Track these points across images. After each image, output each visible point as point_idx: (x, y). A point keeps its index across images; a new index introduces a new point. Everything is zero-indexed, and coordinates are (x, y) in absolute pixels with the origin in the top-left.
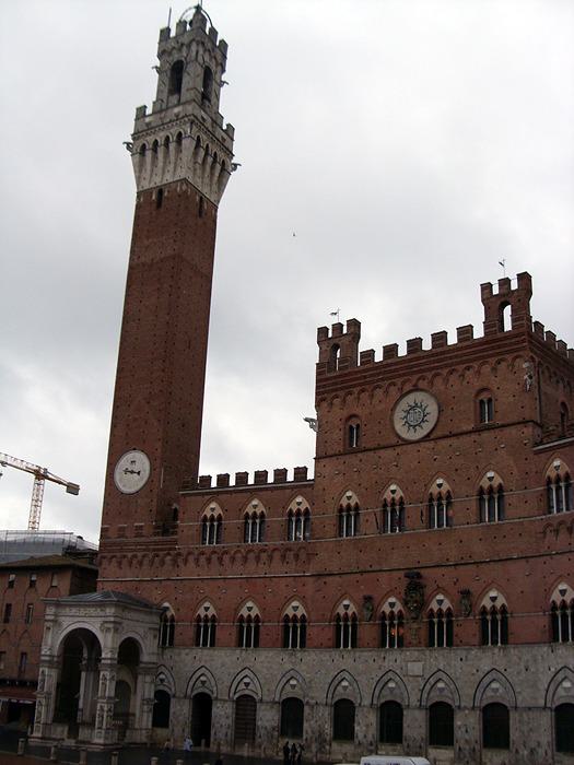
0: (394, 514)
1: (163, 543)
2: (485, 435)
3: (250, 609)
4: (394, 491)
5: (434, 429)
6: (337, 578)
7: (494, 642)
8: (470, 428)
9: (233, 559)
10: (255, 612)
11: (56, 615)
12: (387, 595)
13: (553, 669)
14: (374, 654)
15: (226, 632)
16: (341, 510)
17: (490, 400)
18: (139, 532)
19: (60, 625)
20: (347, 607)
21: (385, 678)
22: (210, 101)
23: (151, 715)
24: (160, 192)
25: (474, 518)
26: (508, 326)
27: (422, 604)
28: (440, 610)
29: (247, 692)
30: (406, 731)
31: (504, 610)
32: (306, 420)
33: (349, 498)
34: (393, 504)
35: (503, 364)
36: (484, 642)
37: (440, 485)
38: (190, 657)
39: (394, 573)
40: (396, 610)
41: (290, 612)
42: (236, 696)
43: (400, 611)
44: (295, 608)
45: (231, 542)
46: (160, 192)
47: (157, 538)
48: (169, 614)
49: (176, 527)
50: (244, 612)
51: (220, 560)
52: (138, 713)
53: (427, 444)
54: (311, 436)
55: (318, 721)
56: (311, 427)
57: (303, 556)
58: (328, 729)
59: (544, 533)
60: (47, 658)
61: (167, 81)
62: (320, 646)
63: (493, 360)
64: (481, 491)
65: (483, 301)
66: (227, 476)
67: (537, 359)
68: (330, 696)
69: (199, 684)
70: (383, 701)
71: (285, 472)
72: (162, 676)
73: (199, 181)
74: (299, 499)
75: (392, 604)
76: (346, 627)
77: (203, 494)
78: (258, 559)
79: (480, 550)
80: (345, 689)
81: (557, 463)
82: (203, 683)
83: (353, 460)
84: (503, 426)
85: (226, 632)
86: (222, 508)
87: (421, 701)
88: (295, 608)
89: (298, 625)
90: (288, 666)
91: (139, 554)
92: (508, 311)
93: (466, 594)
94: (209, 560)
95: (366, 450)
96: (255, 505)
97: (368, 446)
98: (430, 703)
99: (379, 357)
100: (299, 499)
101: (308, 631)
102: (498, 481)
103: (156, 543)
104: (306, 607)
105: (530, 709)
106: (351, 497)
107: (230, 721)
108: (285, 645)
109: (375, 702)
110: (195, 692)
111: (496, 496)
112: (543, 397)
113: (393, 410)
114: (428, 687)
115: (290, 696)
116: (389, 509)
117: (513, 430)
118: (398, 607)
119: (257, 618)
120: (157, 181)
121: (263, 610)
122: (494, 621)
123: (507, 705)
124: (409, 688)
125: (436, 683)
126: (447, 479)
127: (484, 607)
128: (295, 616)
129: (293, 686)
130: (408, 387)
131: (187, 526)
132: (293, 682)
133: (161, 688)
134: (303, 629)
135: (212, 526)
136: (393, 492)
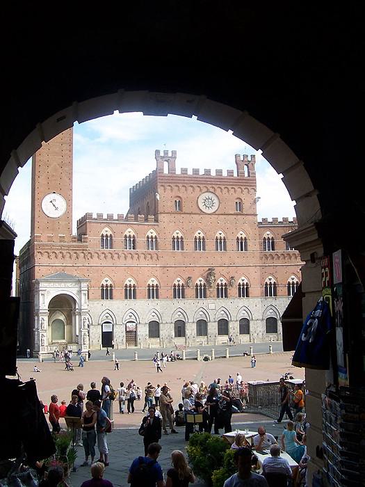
0: (200, 243)
2: (239, 216)
4: (199, 234)
10: (133, 283)
12: (198, 277)
14: (194, 301)
16: (174, 238)
20: (179, 281)
25: (236, 249)
30: (209, 331)
33: (177, 233)
34: (200, 239)
37: (220, 234)
44: (153, 281)
47: (74, 244)
49: (86, 238)
51: (112, 257)
55: (167, 330)
75: (200, 281)
79: (238, 262)
81: (268, 233)
85: (118, 292)
88: (153, 281)
91: (63, 251)
97: (186, 212)
102: (244, 236)
129: (153, 316)
130: (206, 190)
131: (93, 238)
134: (157, 290)
136: (199, 233)
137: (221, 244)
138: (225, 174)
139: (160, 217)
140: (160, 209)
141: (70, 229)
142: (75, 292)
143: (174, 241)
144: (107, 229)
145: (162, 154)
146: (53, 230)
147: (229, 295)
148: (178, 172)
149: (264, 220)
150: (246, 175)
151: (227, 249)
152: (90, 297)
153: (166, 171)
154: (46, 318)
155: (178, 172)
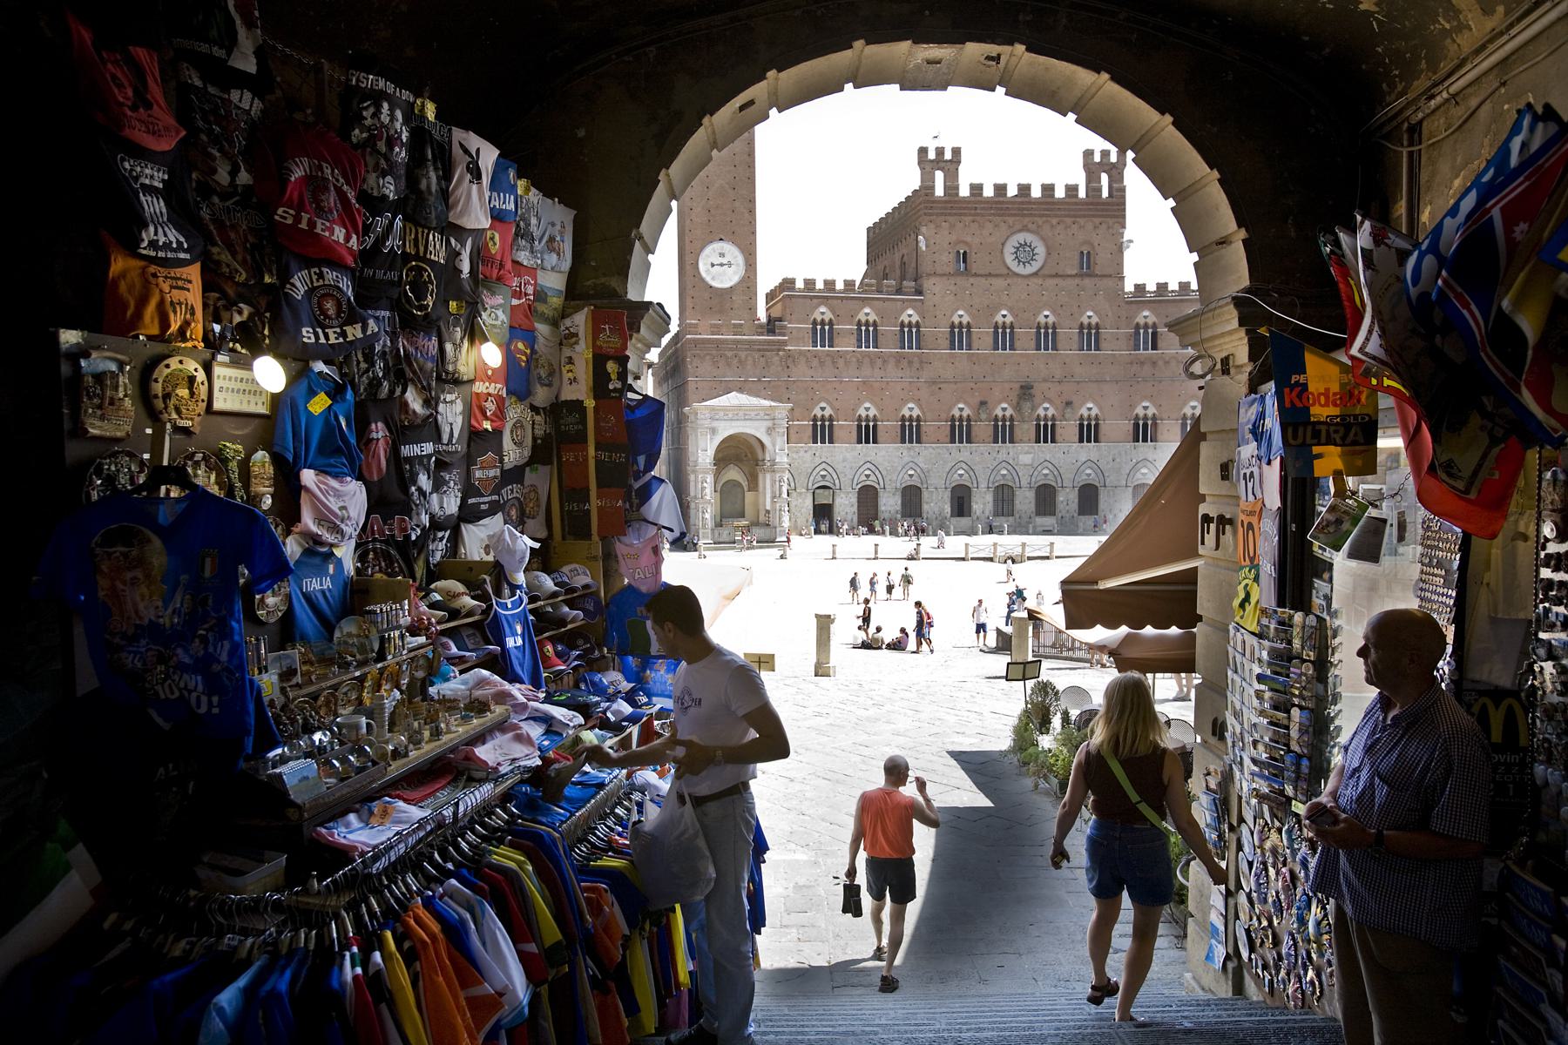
0: (1004, 337)
1: (769, 342)
2: (1087, 282)
3: (867, 409)
4: (1004, 316)
6: (953, 386)
7: (1089, 441)
16: (953, 326)
18: (737, 329)
19: (714, 431)
20: (961, 410)
25: (1076, 346)
27: (1034, 408)
31: (1097, 418)
34: (1004, 327)
35: (1104, 226)
36: (1081, 441)
37: (1046, 316)
38: (810, 453)
39: (1007, 386)
40: (1008, 414)
44: (911, 409)
45: (846, 346)
53: (1035, 280)
57: (916, 365)
58: (948, 509)
62: (938, 441)
63: (1097, 220)
64: (1081, 326)
65: (1085, 166)
66: (833, 283)
74: (910, 312)
75: (1004, 409)
77: (812, 298)
80: (960, 476)
81: (1146, 313)
82: (823, 477)
83: (960, 281)
90: (907, 459)
95: (976, 275)
99: (988, 192)
101: (923, 429)
102: (1095, 320)
103: (760, 342)
104: (920, 407)
106: (962, 316)
107: (855, 509)
108: (903, 442)
117: (1109, 283)
119: (875, 419)
121: (881, 410)
126: (1054, 312)
130: (1018, 227)
134: (918, 426)
135: (823, 330)
137: (1046, 337)
138: (1060, 193)
139: (928, 284)
140: (926, 267)
141: (753, 309)
142: (763, 430)
143: (952, 332)
144: (823, 309)
145: (932, 155)
146: (721, 312)
147: (1058, 437)
148: (964, 192)
149: (1137, 286)
150: (1105, 194)
151: (1059, 346)
152: (793, 436)
153: (939, 191)
154: (710, 479)
155: (964, 192)
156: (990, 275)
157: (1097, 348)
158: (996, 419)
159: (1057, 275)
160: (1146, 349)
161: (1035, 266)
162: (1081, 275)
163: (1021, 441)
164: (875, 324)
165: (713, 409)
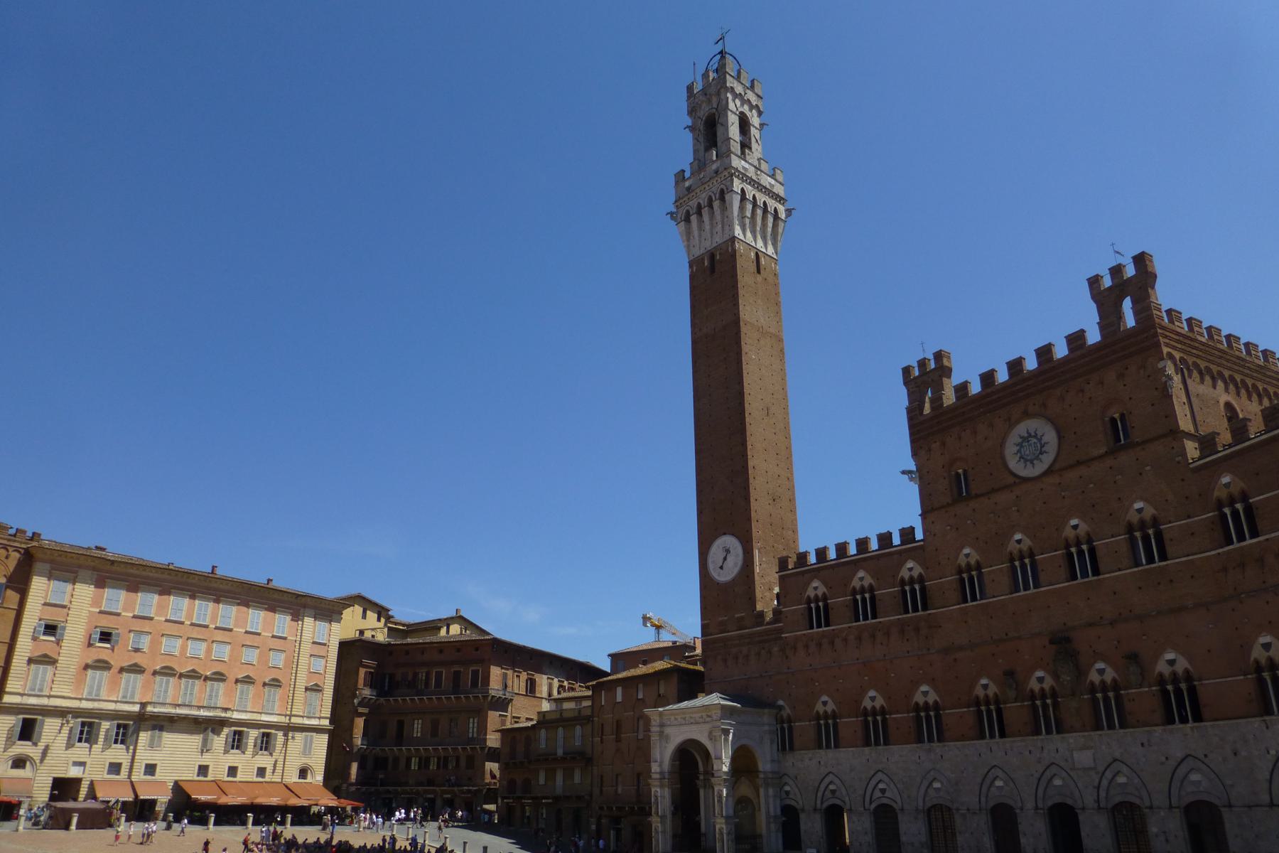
0: (1024, 570)
3: (873, 699)
5: (1055, 461)
7: (1184, 720)
8: (1103, 450)
9: (845, 640)
11: (662, 725)
12: (1033, 669)
13: (1273, 752)
15: (849, 724)
16: (960, 572)
17: (1122, 416)
20: (985, 687)
21: (1048, 774)
22: (750, 148)
23: (780, 835)
24: (712, 256)
26: (1130, 321)
27: (1081, 673)
28: (1103, 682)
29: (885, 801)
31: (1188, 677)
32: (904, 472)
33: (967, 555)
34: (1022, 558)
36: (1170, 721)
41: (919, 698)
42: (873, 806)
43: (1052, 688)
44: (925, 694)
46: (712, 256)
48: (785, 715)
49: (780, 612)
50: (867, 703)
51: (832, 643)
52: (764, 832)
54: (914, 489)
56: (911, 479)
59: (1225, 570)
60: (658, 776)
61: (701, 139)
62: (963, 738)
64: (1130, 529)
65: (1093, 297)
67: (1177, 355)
68: (983, 799)
69: (828, 794)
70: (1050, 803)
71: (889, 535)
72: (787, 788)
73: (749, 234)
75: (1040, 679)
76: (989, 712)
78: (873, 636)
81: (1226, 479)
82: (833, 792)
84: (1144, 442)
86: (825, 583)
87: (1098, 801)
88: (925, 694)
89: (932, 713)
92: (1127, 304)
93: (1133, 657)
94: (819, 645)
95: (977, 496)
96: (862, 578)
98: (1110, 806)
100: (910, 564)
102: (1150, 511)
105: (1249, 807)
108: (920, 740)
109: (1040, 805)
110: (825, 805)
111: (1151, 532)
112: (1193, 399)
113: (1002, 445)
114: (1105, 783)
115: (935, 802)
116: (1017, 563)
118: (1049, 683)
119: (883, 711)
120: (708, 245)
122: (1178, 692)
123: (1216, 802)
124: (1080, 785)
125: (1114, 776)
127: (1161, 675)
128: (926, 703)
129: (937, 790)
132: (937, 785)
133: (788, 802)
134: (938, 717)
136: (1019, 542)
144: (815, 583)
148: (949, 398)
151: (1102, 567)
155: (949, 398)
156: (994, 491)
157: (1163, 557)
158: (1032, 696)
159: (1079, 463)
160: (1241, 538)
161: (1047, 459)
162: (1112, 452)
163: (1072, 730)
164: (871, 589)
165: (661, 714)
